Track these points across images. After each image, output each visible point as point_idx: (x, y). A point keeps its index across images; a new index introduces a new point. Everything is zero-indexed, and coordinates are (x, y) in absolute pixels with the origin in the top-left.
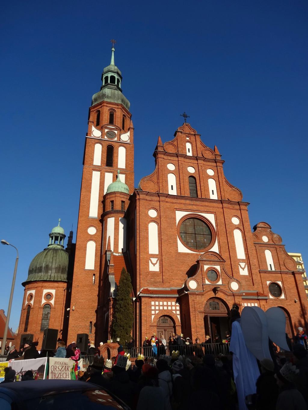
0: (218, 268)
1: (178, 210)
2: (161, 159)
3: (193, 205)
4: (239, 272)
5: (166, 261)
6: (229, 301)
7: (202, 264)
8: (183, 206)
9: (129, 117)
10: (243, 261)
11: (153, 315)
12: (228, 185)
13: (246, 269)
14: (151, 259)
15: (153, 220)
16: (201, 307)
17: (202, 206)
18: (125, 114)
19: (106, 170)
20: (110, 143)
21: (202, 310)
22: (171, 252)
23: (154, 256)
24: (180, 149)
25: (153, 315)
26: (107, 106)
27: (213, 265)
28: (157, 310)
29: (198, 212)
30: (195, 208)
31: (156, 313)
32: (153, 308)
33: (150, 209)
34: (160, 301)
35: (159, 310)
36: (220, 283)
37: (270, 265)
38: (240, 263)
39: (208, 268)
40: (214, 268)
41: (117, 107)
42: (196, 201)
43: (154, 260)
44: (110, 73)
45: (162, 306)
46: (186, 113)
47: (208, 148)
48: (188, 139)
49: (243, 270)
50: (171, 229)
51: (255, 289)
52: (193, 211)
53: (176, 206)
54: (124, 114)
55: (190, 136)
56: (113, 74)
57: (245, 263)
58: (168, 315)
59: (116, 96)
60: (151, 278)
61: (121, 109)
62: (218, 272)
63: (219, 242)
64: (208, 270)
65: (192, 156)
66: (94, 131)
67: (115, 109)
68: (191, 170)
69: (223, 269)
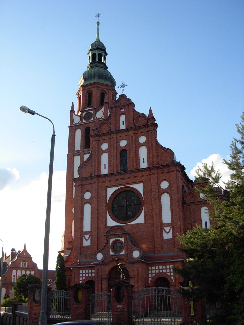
0: (122, 239)
1: (109, 187)
2: (95, 142)
3: (122, 179)
4: (162, 236)
5: (94, 236)
7: (108, 238)
10: (168, 225)
11: (81, 280)
12: (159, 148)
13: (171, 233)
14: (85, 235)
15: (87, 202)
17: (130, 178)
18: (102, 88)
19: (84, 153)
20: (87, 125)
23: (87, 233)
24: (112, 126)
25: (81, 280)
28: (84, 277)
29: (127, 184)
31: (83, 279)
32: (81, 275)
33: (85, 192)
34: (87, 270)
35: (85, 276)
36: (123, 252)
37: (206, 222)
38: (164, 228)
40: (119, 240)
42: (125, 174)
43: (87, 236)
45: (87, 273)
46: (123, 83)
47: (140, 114)
48: (123, 110)
49: (168, 234)
50: (101, 207)
52: (122, 185)
54: (101, 89)
55: (124, 107)
57: (170, 227)
58: (92, 280)
59: (93, 76)
63: (145, 210)
64: (114, 242)
65: (125, 128)
66: (74, 118)
67: (92, 89)
68: (123, 143)
69: (126, 240)
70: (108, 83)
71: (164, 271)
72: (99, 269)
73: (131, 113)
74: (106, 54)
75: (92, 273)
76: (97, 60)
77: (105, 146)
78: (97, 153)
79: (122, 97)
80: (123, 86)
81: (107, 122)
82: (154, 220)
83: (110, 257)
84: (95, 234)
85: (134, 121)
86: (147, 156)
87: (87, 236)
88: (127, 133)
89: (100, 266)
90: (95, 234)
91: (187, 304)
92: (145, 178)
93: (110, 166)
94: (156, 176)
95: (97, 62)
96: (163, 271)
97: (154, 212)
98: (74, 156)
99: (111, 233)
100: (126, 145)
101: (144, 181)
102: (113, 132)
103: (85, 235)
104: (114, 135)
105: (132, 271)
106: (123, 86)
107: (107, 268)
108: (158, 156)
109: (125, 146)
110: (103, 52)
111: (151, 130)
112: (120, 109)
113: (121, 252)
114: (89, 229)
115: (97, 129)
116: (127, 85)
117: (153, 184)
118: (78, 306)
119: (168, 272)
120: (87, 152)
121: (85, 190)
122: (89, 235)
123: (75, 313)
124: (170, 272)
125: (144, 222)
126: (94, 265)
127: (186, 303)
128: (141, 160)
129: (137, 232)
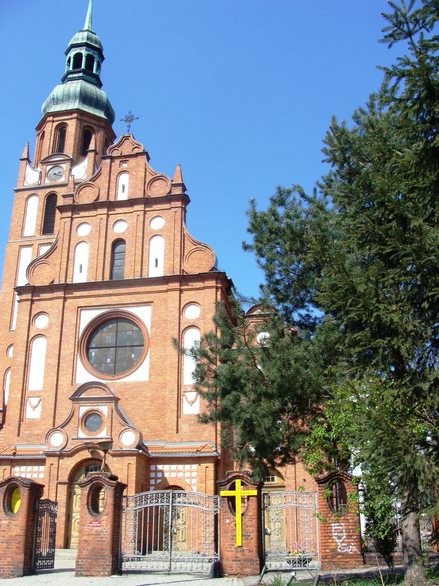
0: (104, 409)
2: (66, 220)
6: (114, 464)
8: (94, 301)
9: (99, 126)
16: (64, 474)
18: (89, 122)
19: (42, 243)
21: (65, 479)
22: (62, 385)
23: (35, 394)
26: (53, 121)
27: (95, 404)
30: (115, 300)
39: (88, 412)
41: (70, 117)
44: (73, 49)
45: (29, 472)
46: (131, 114)
47: (158, 175)
48: (125, 165)
51: (203, 439)
53: (82, 302)
54: (85, 124)
56: (77, 51)
59: (71, 95)
60: (26, 430)
61: (77, 118)
62: (104, 415)
63: (150, 357)
67: (67, 122)
70: (101, 114)
71: (180, 475)
72: (52, 464)
73: (141, 171)
74: (102, 58)
75: (38, 472)
76: (83, 67)
77: (84, 231)
78: (67, 241)
79: (125, 139)
80: (130, 119)
81: (93, 183)
82: (168, 378)
83: (77, 440)
84: (51, 397)
85: (146, 185)
86: (165, 255)
87: (34, 401)
88: (130, 209)
89: (56, 458)
90: (51, 397)
91: (229, 524)
92: (156, 297)
93: (90, 268)
94: (178, 293)
95: (83, 71)
96: (177, 476)
97: (168, 362)
98: (20, 246)
99: (83, 396)
100: (126, 231)
101: (152, 302)
102: (102, 205)
103: (30, 398)
104: (105, 211)
105: (119, 471)
106: (130, 119)
107: (70, 463)
108: (184, 257)
109: (123, 233)
110: (97, 53)
111: (175, 207)
112: (121, 161)
113: (99, 433)
114: (40, 388)
115: (72, 196)
116: (137, 118)
117: (171, 309)
118: (10, 523)
119: (188, 478)
120: (46, 242)
121: (38, 311)
122: (38, 399)
123: (2, 537)
124: (191, 478)
125: (146, 378)
126: (44, 457)
127: (228, 521)
128: (152, 262)
129: (133, 398)
